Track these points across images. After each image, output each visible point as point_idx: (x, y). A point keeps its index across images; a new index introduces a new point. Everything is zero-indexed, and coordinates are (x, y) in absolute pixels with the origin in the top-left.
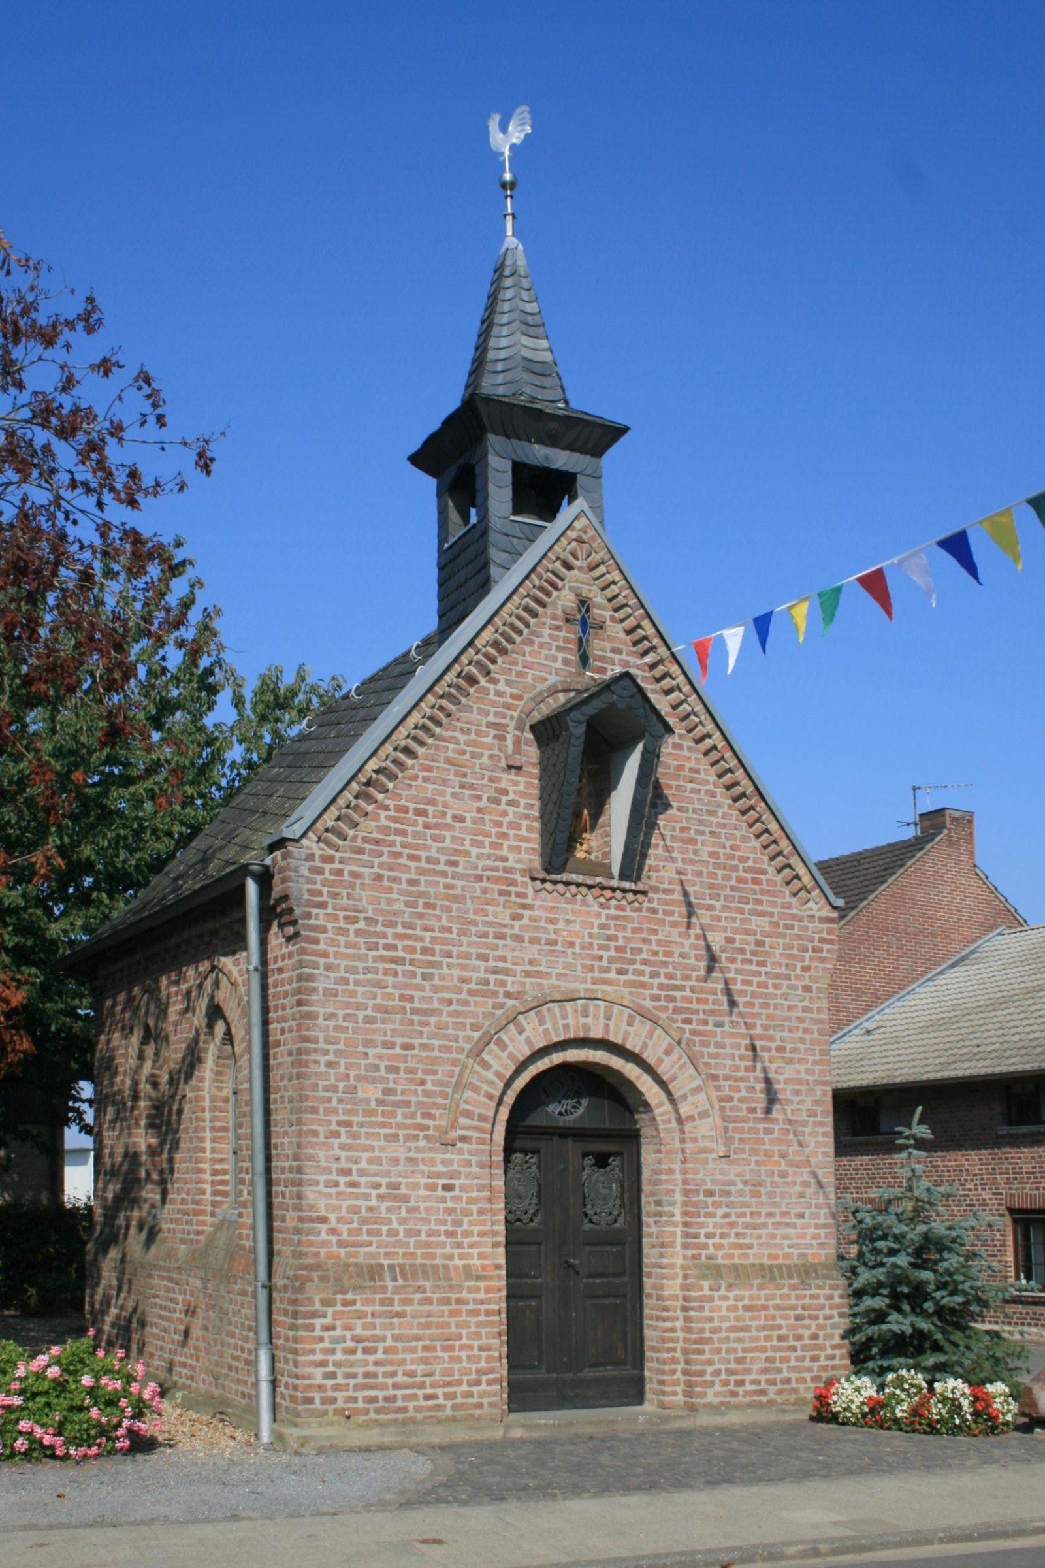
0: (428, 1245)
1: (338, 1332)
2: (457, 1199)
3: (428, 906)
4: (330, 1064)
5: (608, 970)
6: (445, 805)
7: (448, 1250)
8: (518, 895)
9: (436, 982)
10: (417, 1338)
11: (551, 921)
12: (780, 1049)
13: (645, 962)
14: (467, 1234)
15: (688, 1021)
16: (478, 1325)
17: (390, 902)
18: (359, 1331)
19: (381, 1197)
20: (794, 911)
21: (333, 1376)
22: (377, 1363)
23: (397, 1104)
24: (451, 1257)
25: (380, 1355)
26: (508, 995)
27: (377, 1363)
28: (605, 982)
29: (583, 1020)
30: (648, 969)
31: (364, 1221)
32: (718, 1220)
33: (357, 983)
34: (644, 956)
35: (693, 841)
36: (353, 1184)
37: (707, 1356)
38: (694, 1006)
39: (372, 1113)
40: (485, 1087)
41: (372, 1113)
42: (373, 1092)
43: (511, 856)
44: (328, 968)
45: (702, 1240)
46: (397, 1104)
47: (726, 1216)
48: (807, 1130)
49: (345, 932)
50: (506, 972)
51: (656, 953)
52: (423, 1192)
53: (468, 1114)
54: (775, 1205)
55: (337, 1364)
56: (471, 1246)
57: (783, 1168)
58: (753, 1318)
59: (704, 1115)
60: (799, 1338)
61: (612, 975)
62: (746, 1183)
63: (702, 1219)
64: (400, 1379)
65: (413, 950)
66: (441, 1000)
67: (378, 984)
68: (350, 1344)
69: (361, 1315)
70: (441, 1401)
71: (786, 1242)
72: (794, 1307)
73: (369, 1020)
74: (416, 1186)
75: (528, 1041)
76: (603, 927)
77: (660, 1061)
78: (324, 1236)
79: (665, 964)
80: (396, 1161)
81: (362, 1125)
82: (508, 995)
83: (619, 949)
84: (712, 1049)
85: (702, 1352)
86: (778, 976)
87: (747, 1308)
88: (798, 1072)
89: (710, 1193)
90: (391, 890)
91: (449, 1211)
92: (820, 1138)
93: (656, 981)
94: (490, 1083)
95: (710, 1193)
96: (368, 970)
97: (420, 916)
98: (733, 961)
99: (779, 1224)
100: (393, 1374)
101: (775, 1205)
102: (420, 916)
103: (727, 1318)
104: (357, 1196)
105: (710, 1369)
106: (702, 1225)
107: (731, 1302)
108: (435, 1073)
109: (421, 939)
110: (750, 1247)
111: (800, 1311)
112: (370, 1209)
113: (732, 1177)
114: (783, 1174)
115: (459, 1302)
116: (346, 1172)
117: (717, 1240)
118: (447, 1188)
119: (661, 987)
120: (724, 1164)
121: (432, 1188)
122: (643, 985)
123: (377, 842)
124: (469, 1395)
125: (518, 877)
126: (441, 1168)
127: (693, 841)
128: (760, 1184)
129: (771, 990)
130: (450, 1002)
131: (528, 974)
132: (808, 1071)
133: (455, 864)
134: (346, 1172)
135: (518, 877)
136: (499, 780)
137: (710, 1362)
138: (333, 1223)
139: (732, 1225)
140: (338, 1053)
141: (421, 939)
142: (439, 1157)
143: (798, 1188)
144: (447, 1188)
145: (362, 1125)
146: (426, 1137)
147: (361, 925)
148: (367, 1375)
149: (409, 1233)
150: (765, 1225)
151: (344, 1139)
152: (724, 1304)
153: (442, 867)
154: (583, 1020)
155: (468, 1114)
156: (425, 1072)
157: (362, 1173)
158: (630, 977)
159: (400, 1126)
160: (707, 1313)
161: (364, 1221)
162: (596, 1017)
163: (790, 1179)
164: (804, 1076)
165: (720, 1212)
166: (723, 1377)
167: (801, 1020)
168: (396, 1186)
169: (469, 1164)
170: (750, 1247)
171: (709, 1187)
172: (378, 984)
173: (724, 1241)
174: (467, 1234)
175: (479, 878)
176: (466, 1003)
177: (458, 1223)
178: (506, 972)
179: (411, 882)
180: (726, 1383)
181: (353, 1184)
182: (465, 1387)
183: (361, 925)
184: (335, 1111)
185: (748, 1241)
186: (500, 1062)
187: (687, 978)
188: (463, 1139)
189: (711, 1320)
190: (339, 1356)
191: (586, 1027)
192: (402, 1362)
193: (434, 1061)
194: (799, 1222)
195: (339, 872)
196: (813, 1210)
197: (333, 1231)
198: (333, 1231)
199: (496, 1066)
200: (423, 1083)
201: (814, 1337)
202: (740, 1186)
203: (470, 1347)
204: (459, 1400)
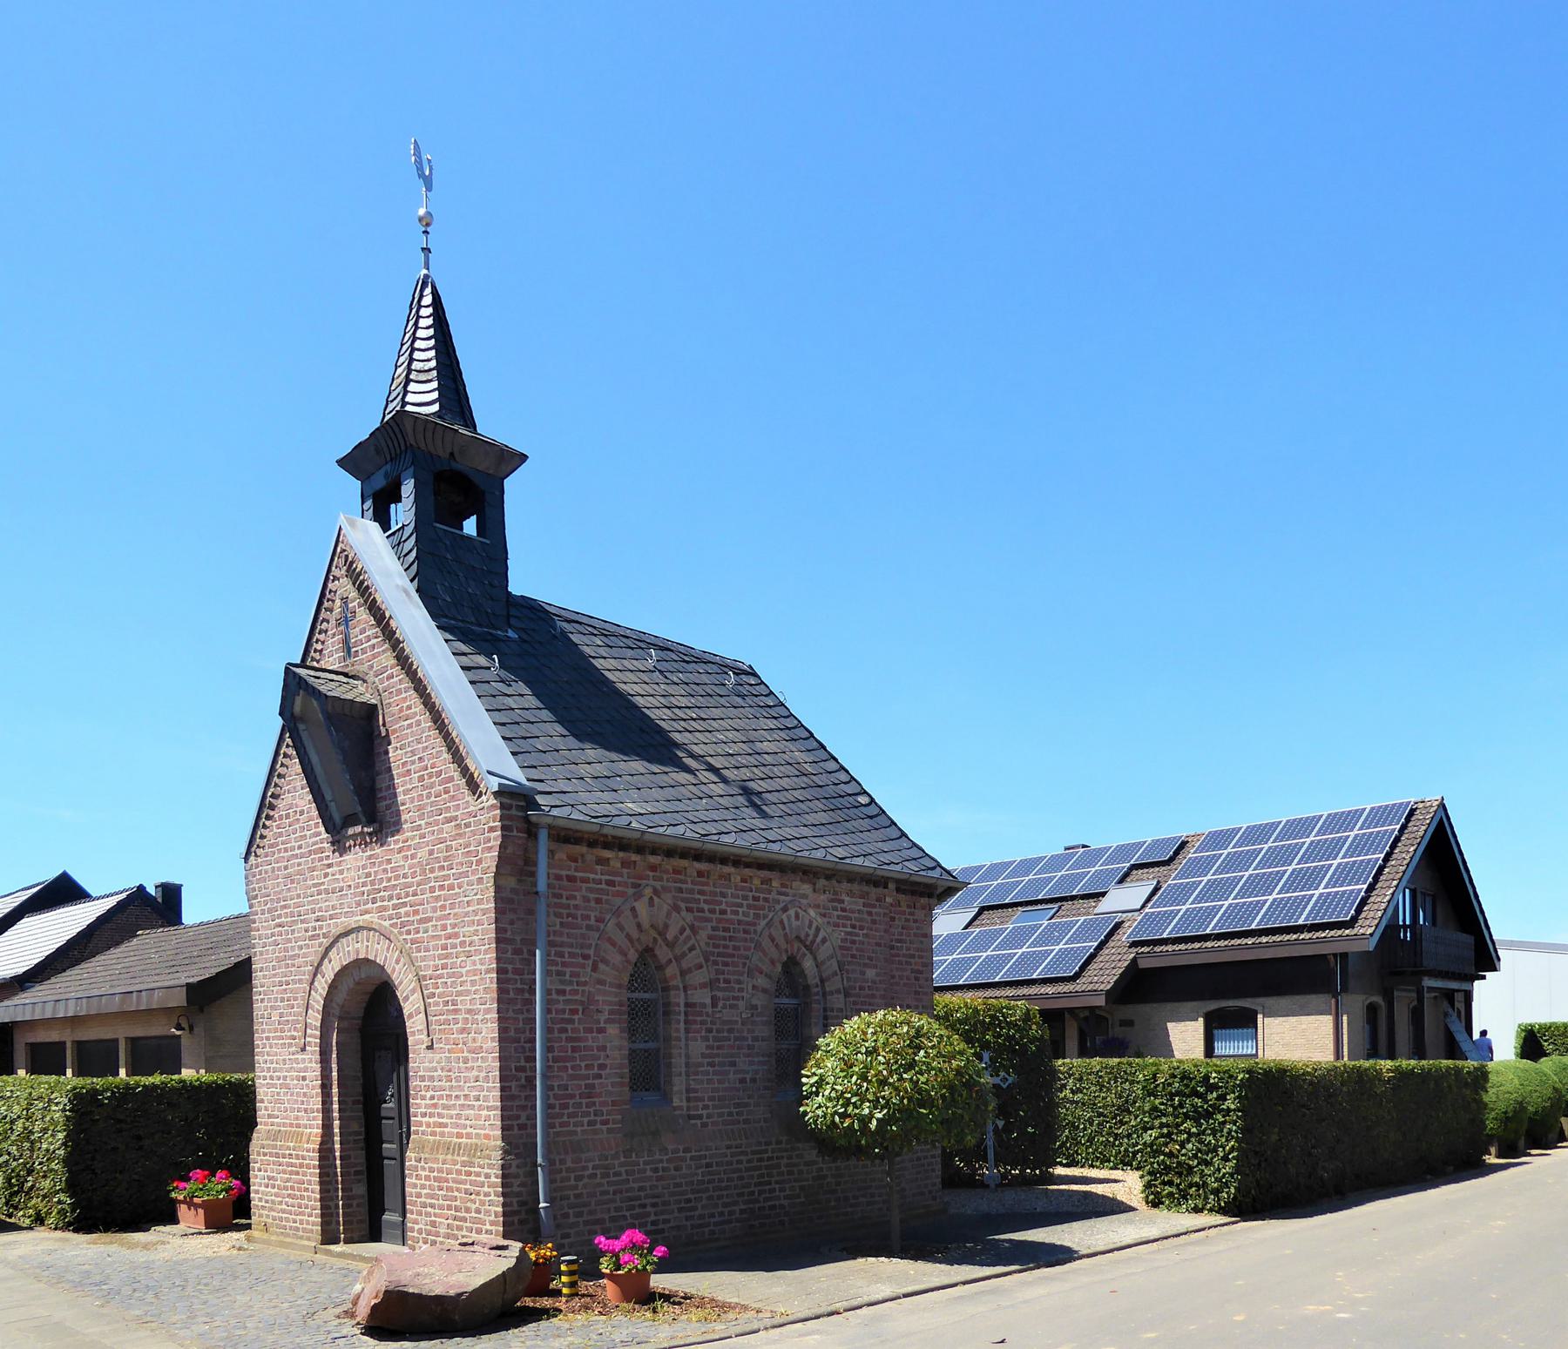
12: (463, 944)
15: (408, 933)
47: (432, 1098)
48: (480, 1017)
60: (468, 1210)
72: (464, 1182)
87: (436, 1179)
88: (474, 963)
95: (423, 1079)
98: (432, 871)
101: (460, 1088)
103: (423, 1187)
110: (445, 1126)
114: (466, 1061)
120: (430, 1054)
142: (300, 1057)
170: (445, 1126)
201: (478, 1211)
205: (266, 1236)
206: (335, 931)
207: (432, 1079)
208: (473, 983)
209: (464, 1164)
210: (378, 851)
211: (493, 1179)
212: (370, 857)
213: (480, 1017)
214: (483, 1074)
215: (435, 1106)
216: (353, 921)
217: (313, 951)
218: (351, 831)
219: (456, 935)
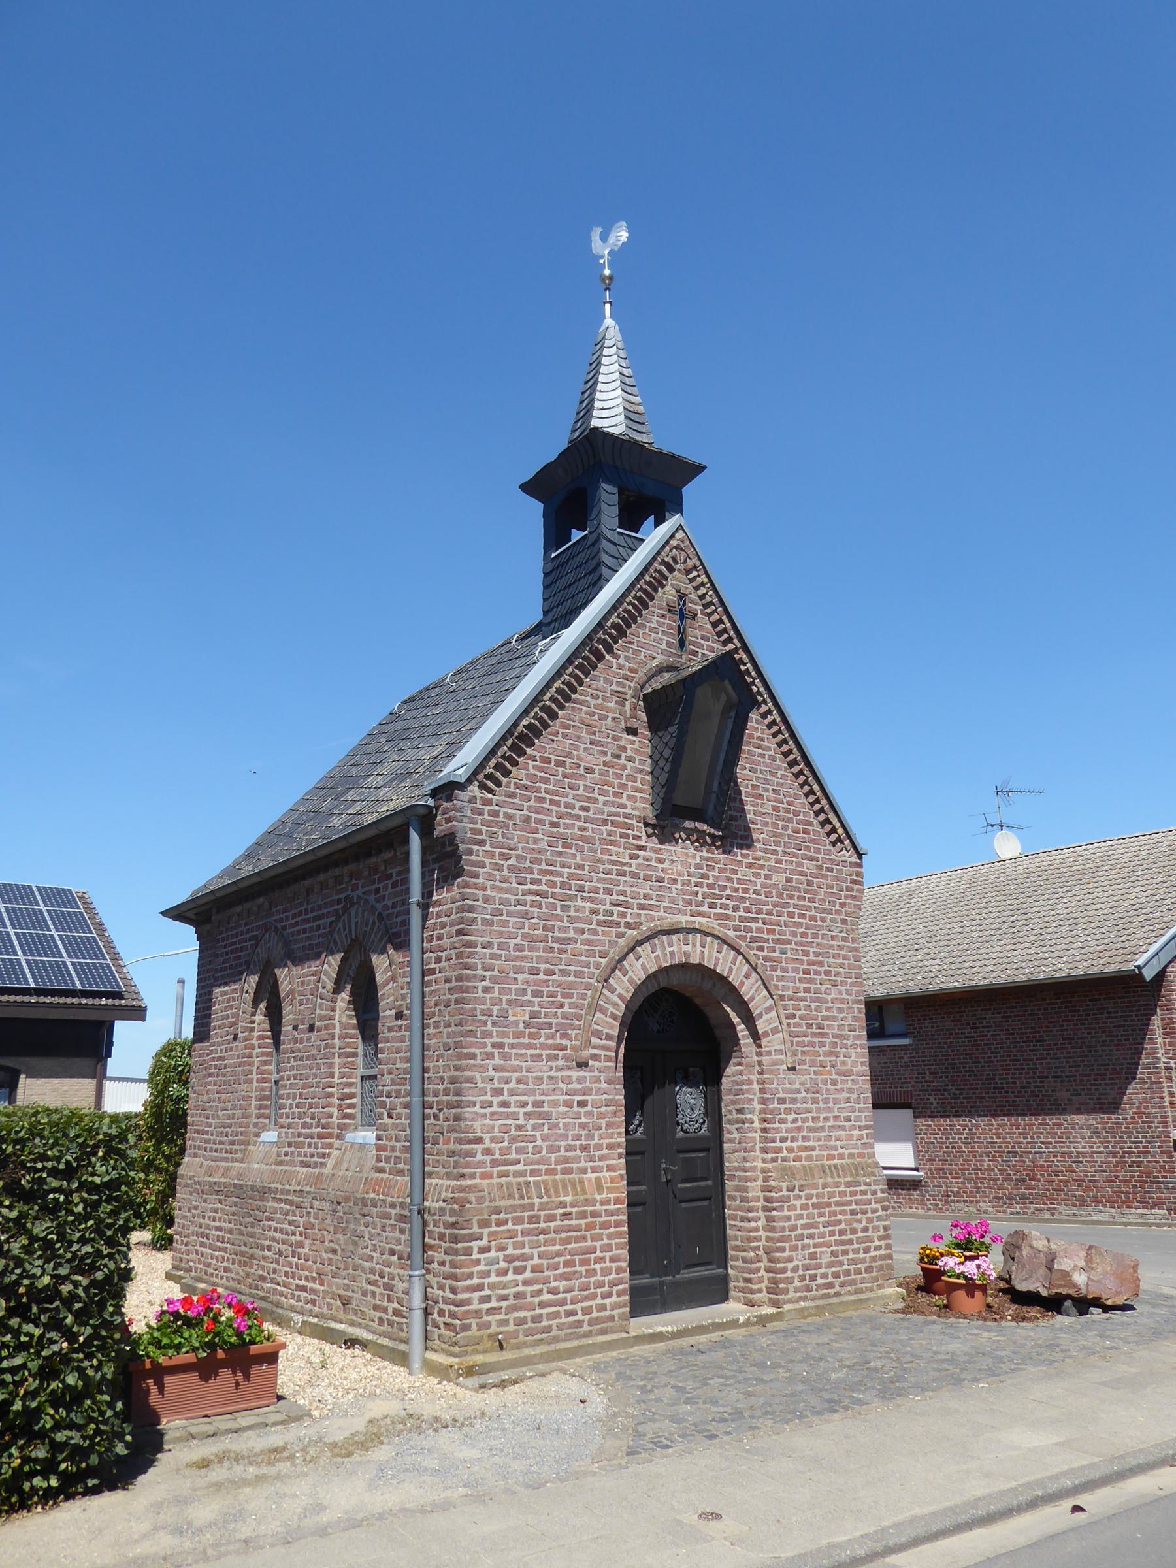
0: (566, 1160)
1: (492, 1254)
2: (590, 1114)
3: (565, 845)
4: (486, 990)
5: (701, 904)
6: (579, 758)
7: (583, 1164)
8: (635, 837)
9: (572, 913)
10: (559, 1254)
11: (660, 861)
12: (827, 973)
13: (729, 898)
14: (598, 1147)
15: (761, 949)
16: (609, 1237)
17: (536, 841)
18: (510, 1251)
19: (528, 1116)
20: (833, 857)
21: (487, 1299)
22: (526, 1283)
23: (541, 1026)
24: (584, 1171)
25: (528, 1274)
26: (628, 925)
27: (526, 1283)
28: (700, 914)
29: (685, 948)
30: (731, 904)
31: (513, 1140)
32: (789, 1125)
33: (509, 914)
34: (728, 892)
35: (760, 797)
36: (505, 1104)
37: (787, 1254)
38: (765, 936)
39: (520, 1035)
40: (611, 1009)
41: (520, 1035)
42: (520, 1015)
43: (629, 804)
44: (486, 900)
45: (778, 1144)
46: (541, 1026)
47: (795, 1121)
48: (849, 1043)
49: (499, 868)
50: (626, 905)
51: (736, 890)
52: (562, 1109)
53: (598, 1034)
54: (829, 1110)
55: (492, 1287)
56: (602, 1158)
57: (834, 1077)
58: (821, 1215)
59: (775, 1031)
60: (854, 1231)
61: (705, 909)
62: (807, 1091)
63: (777, 1125)
64: (546, 1297)
65: (553, 884)
66: (576, 930)
67: (527, 916)
68: (503, 1264)
69: (511, 1235)
70: (579, 1317)
71: (839, 1143)
72: (849, 1203)
73: (518, 947)
74: (555, 1104)
75: (643, 966)
76: (697, 866)
77: (742, 983)
78: (479, 1157)
79: (743, 899)
80: (539, 1080)
81: (512, 1046)
82: (628, 925)
83: (709, 886)
84: (779, 973)
85: (783, 1250)
86: (824, 911)
87: (815, 1206)
88: (840, 993)
89: (782, 1101)
90: (536, 831)
91: (583, 1126)
92: (859, 1050)
93: (737, 914)
94: (615, 1005)
95: (782, 1101)
96: (519, 903)
97: (560, 854)
98: (791, 897)
99: (833, 1127)
100: (540, 1292)
101: (829, 1110)
102: (560, 854)
103: (800, 1217)
104: (508, 1116)
105: (790, 1265)
106: (778, 1130)
107: (803, 1201)
108: (570, 996)
109: (560, 875)
110: (813, 1149)
111: (854, 1207)
112: (519, 1128)
113: (797, 1086)
114: (834, 1083)
115: (594, 1214)
116: (499, 1092)
117: (788, 1144)
118: (582, 1104)
119: (742, 919)
120: (791, 1075)
121: (568, 1104)
122: (728, 917)
123: (526, 788)
124: (602, 1308)
125: (634, 822)
126: (576, 1086)
127: (760, 797)
128: (818, 1092)
129: (819, 923)
130: (583, 932)
131: (642, 907)
132: (848, 993)
133: (586, 809)
134: (499, 1092)
135: (634, 822)
136: (619, 739)
137: (790, 1260)
138: (488, 1144)
139: (799, 1129)
140: (494, 980)
141: (560, 875)
142: (575, 1074)
143: (845, 1095)
144: (582, 1104)
145: (512, 1046)
146: (567, 1059)
147: (513, 861)
148: (518, 1296)
149: (551, 1149)
150: (822, 1129)
151: (497, 1061)
152: (798, 1203)
153: (576, 812)
154: (685, 948)
155: (598, 1034)
156: (564, 996)
157: (512, 1093)
158: (718, 910)
159: (543, 1046)
160: (786, 1213)
161: (513, 1140)
162: (694, 945)
163: (839, 1087)
164: (845, 996)
165: (790, 1117)
166: (801, 1272)
167: (841, 948)
168: (539, 1104)
169: (598, 1080)
170: (813, 1149)
171: (781, 1095)
172: (527, 916)
173: (795, 1145)
174: (598, 1147)
175: (605, 822)
176: (595, 932)
177: (590, 1137)
178: (626, 905)
179: (554, 825)
180: (802, 1278)
181: (505, 1104)
182: (599, 1301)
183: (513, 861)
184: (490, 1035)
185: (811, 1143)
186: (624, 986)
187: (760, 912)
188: (595, 1057)
189: (789, 1218)
190: (493, 1279)
191: (687, 954)
192: (546, 1281)
193: (571, 985)
194: (847, 1124)
195: (495, 814)
196: (857, 1113)
197: (488, 1152)
198: (488, 1152)
199: (619, 990)
200: (561, 1006)
201: (865, 1230)
202: (804, 1094)
203: (602, 1259)
204: (595, 1314)
205: (507, 1355)
206: (658, 924)
207: (793, 1101)
208: (840, 1010)
209: (848, 1185)
210: (717, 855)
211: (880, 1195)
212: (708, 859)
213: (849, 1043)
214: (855, 1096)
215: (799, 1129)
216: (684, 920)
217: (611, 941)
218: (688, 824)
219: (820, 964)
